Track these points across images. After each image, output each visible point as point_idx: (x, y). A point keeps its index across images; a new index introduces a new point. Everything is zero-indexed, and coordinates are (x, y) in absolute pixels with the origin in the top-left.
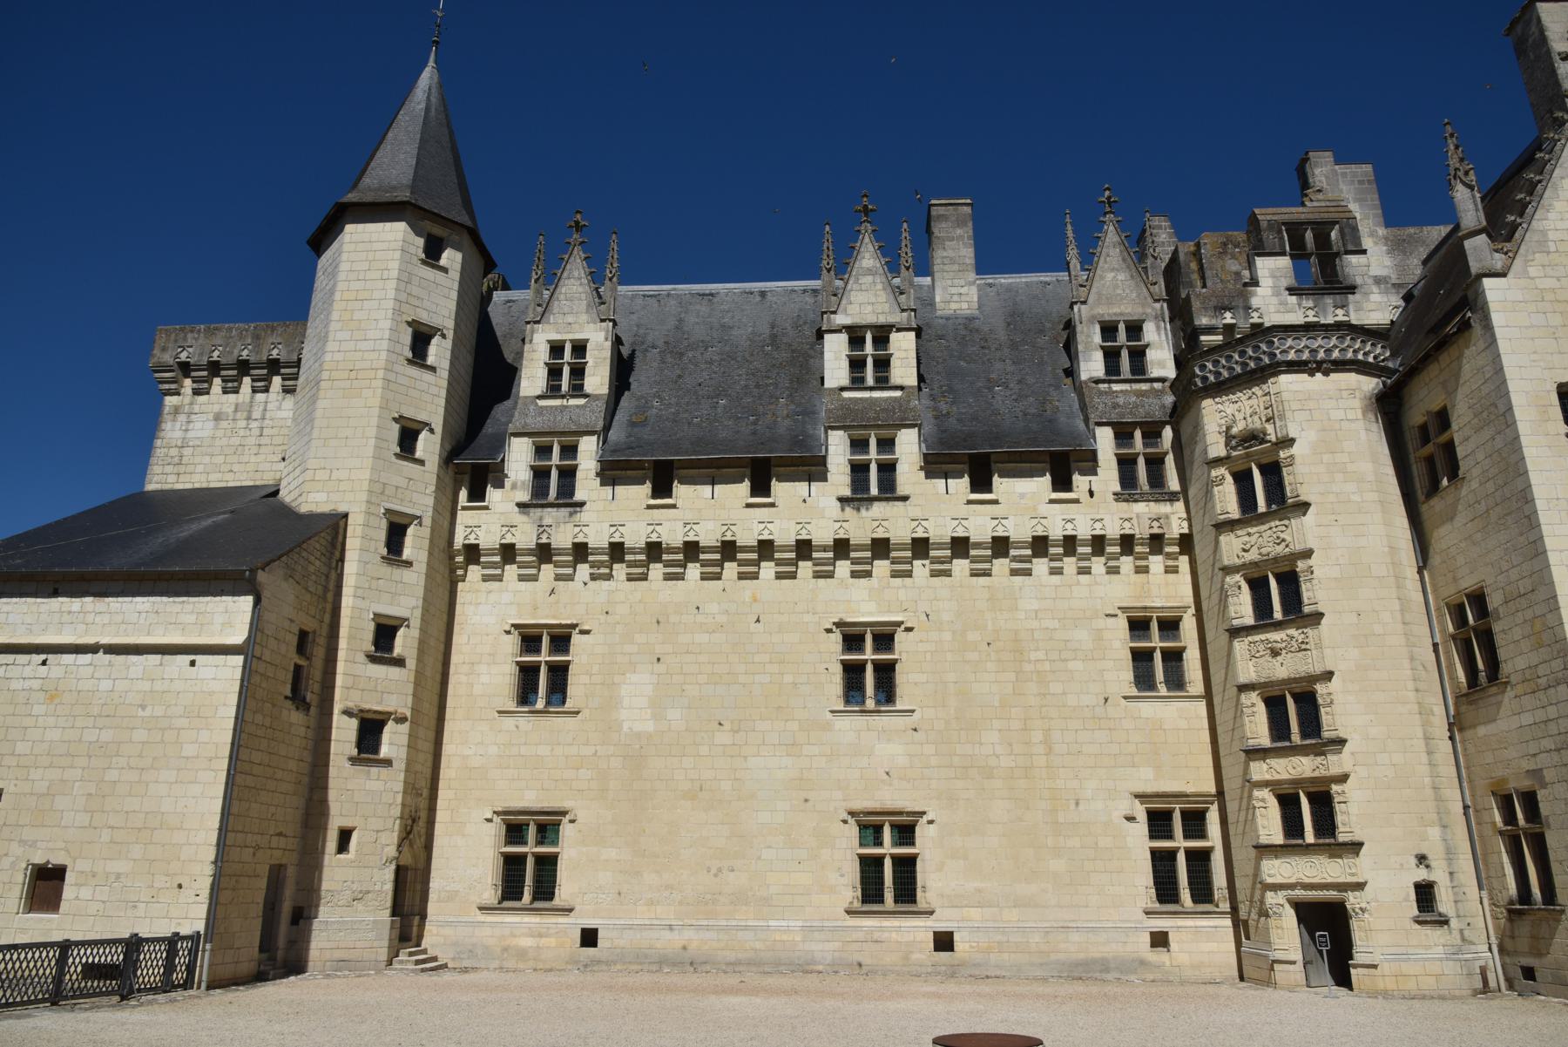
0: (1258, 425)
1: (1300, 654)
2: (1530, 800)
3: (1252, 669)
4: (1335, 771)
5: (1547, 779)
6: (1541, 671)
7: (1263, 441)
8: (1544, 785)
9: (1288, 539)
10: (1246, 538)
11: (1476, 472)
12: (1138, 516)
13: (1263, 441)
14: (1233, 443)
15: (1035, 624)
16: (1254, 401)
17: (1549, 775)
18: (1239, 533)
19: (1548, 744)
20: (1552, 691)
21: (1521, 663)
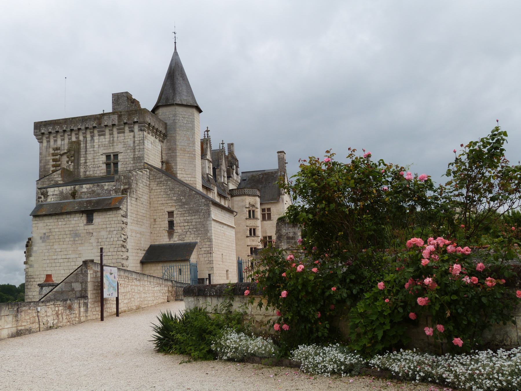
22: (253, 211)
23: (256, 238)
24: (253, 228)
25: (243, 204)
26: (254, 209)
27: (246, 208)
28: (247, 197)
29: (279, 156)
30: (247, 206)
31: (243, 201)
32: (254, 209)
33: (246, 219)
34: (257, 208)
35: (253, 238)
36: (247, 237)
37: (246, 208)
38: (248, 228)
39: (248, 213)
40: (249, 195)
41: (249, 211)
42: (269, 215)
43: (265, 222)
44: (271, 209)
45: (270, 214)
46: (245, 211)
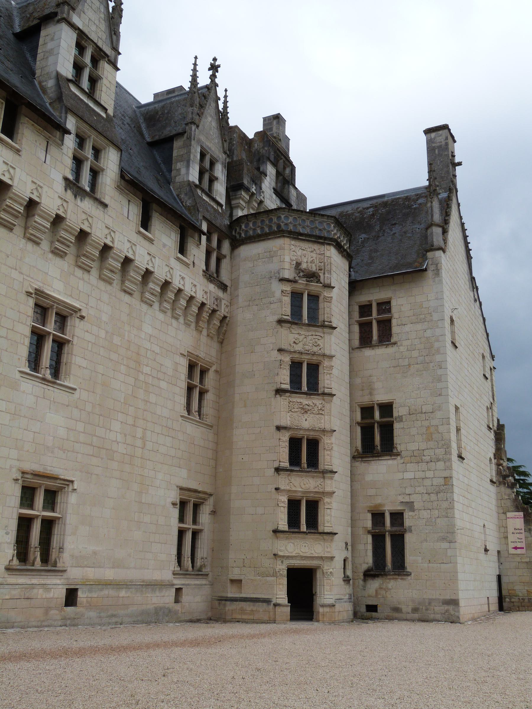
0: (314, 269)
1: (317, 416)
2: (398, 517)
3: (289, 418)
4: (328, 489)
5: (416, 507)
6: (426, 453)
7: (318, 281)
8: (412, 509)
9: (322, 346)
10: (297, 336)
11: (405, 343)
12: (210, 291)
13: (318, 281)
14: (301, 274)
15: (148, 345)
16: (314, 255)
17: (416, 506)
18: (293, 331)
19: (421, 489)
20: (433, 464)
21: (413, 447)
22: (314, 298)
23: (317, 401)
24: (306, 359)
25: (273, 266)
26: (314, 287)
27: (282, 280)
28: (285, 243)
29: (429, 142)
30: (288, 274)
31: (271, 256)
32: (314, 287)
33: (280, 322)
34: (329, 287)
35: (305, 401)
36: (279, 392)
37: (282, 280)
38: (287, 359)
39: (287, 300)
40: (296, 235)
41: (296, 297)
42: (386, 327)
43: (368, 352)
44: (393, 303)
45: (389, 321)
46: (278, 294)
